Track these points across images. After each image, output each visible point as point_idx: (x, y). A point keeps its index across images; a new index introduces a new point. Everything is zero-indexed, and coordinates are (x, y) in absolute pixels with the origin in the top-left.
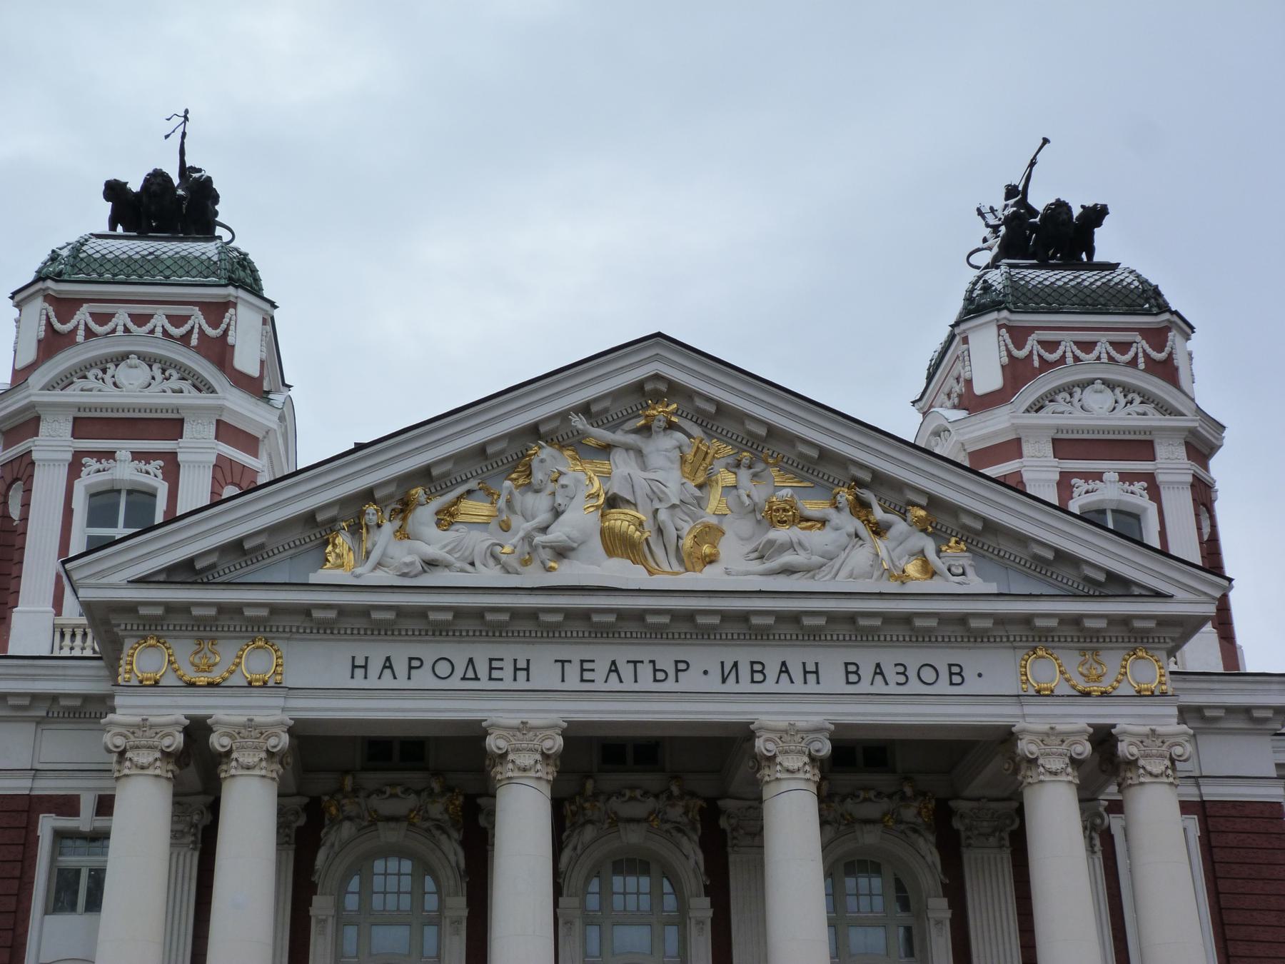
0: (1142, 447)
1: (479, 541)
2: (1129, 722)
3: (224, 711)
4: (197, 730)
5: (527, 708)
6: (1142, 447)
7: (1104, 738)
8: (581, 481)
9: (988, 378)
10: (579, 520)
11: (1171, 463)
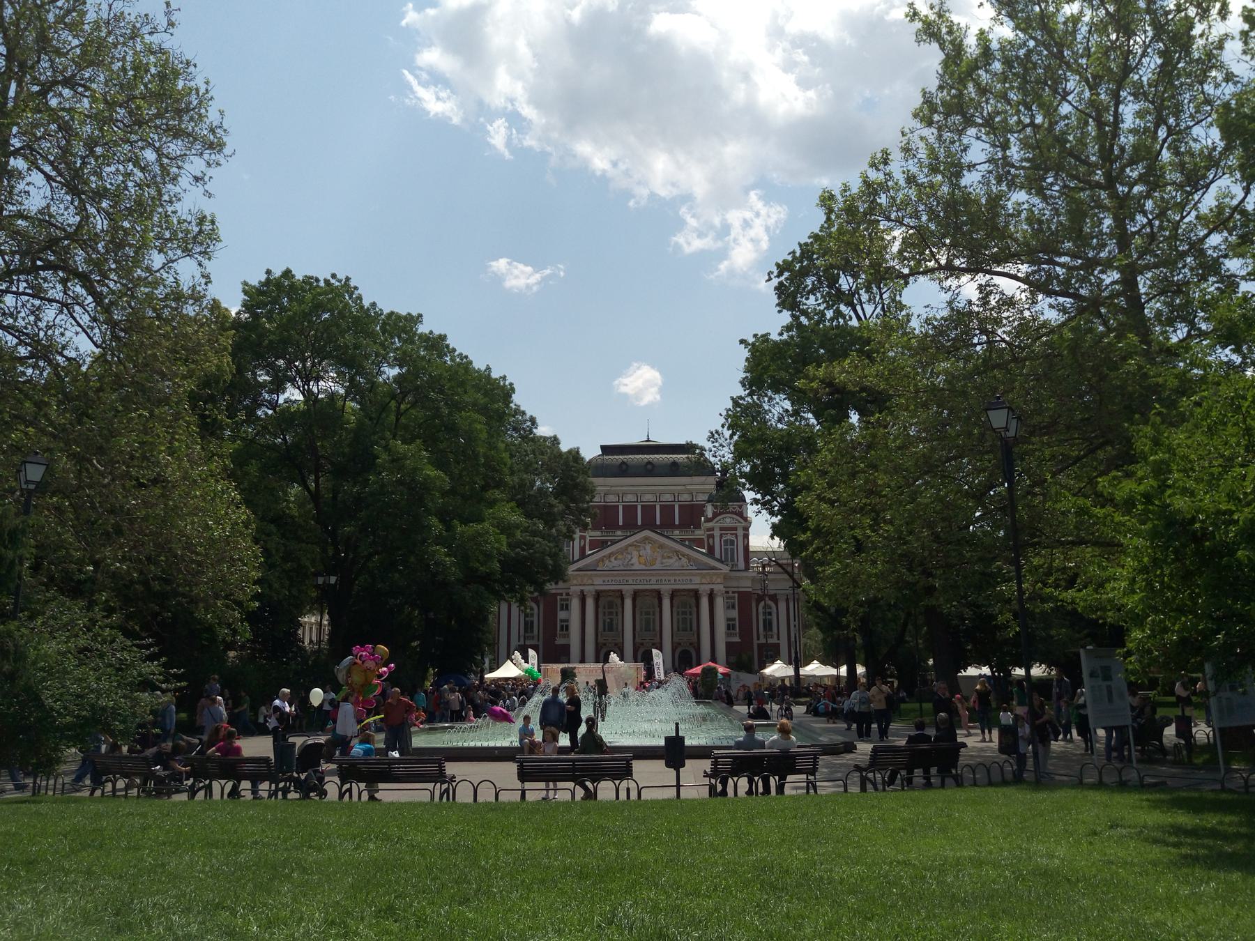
0: (735, 529)
1: (619, 562)
2: (716, 588)
3: (586, 588)
4: (582, 591)
5: (628, 589)
6: (735, 529)
7: (712, 590)
8: (635, 553)
9: (710, 515)
10: (635, 560)
11: (740, 532)
